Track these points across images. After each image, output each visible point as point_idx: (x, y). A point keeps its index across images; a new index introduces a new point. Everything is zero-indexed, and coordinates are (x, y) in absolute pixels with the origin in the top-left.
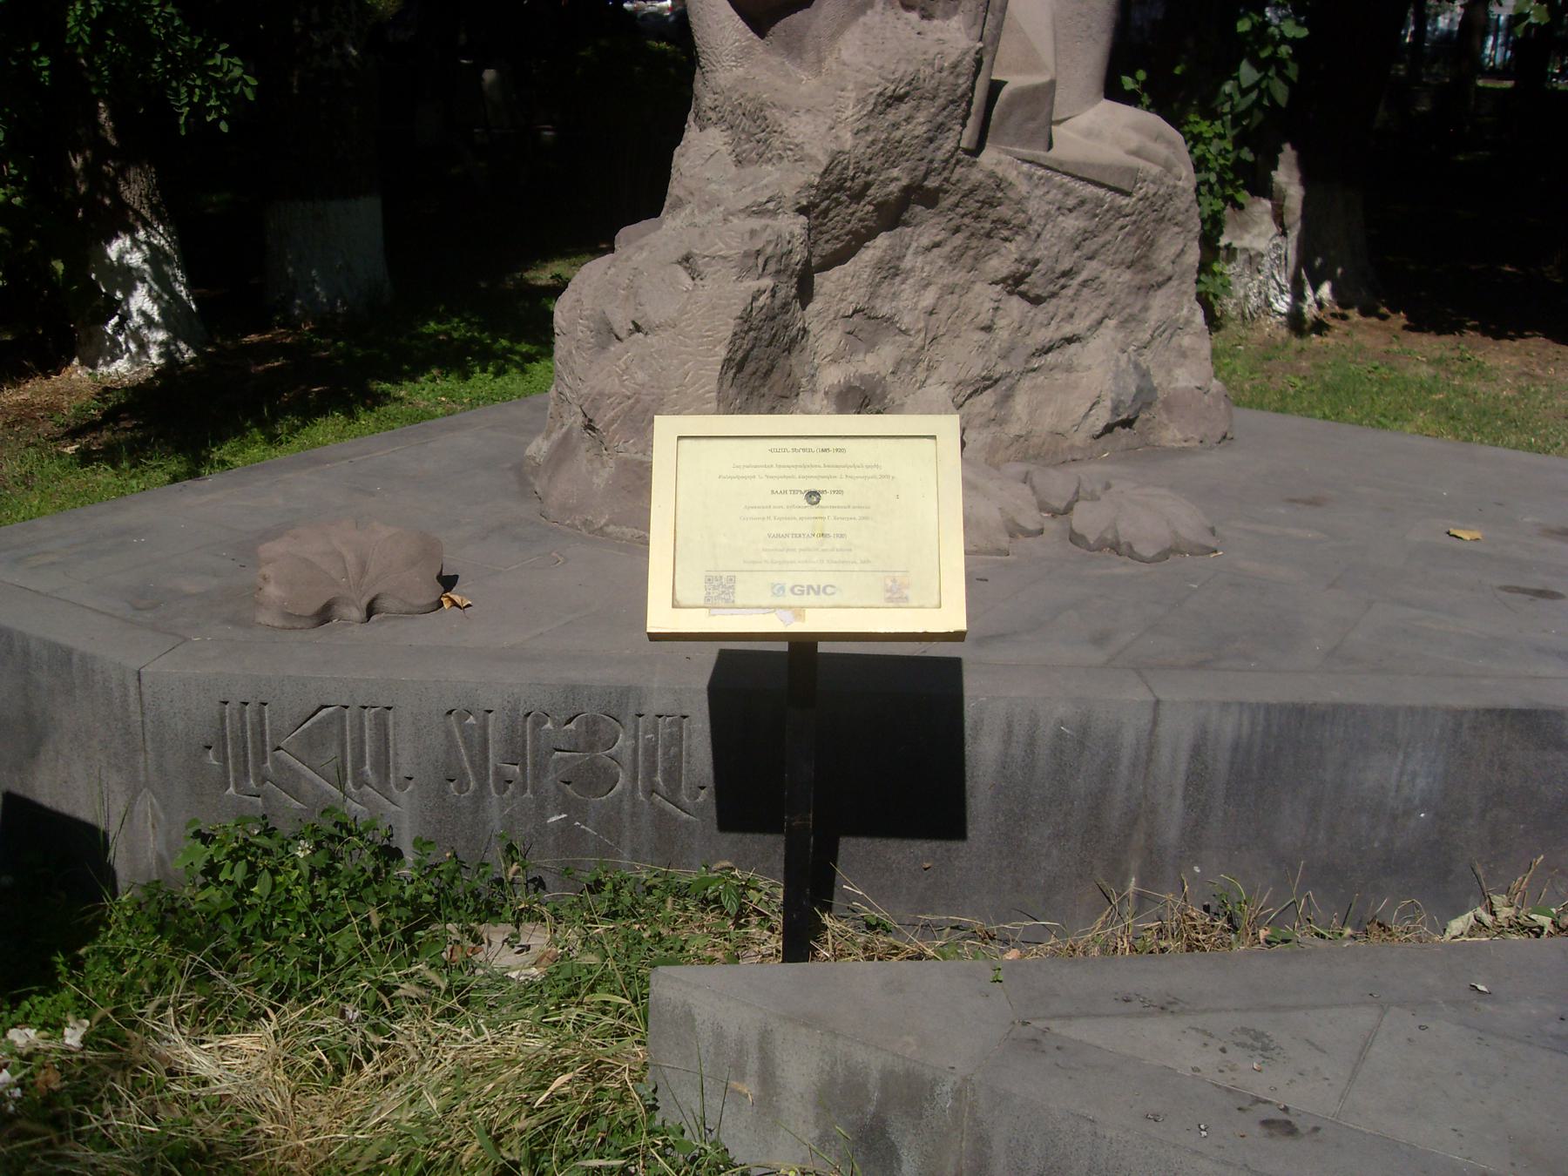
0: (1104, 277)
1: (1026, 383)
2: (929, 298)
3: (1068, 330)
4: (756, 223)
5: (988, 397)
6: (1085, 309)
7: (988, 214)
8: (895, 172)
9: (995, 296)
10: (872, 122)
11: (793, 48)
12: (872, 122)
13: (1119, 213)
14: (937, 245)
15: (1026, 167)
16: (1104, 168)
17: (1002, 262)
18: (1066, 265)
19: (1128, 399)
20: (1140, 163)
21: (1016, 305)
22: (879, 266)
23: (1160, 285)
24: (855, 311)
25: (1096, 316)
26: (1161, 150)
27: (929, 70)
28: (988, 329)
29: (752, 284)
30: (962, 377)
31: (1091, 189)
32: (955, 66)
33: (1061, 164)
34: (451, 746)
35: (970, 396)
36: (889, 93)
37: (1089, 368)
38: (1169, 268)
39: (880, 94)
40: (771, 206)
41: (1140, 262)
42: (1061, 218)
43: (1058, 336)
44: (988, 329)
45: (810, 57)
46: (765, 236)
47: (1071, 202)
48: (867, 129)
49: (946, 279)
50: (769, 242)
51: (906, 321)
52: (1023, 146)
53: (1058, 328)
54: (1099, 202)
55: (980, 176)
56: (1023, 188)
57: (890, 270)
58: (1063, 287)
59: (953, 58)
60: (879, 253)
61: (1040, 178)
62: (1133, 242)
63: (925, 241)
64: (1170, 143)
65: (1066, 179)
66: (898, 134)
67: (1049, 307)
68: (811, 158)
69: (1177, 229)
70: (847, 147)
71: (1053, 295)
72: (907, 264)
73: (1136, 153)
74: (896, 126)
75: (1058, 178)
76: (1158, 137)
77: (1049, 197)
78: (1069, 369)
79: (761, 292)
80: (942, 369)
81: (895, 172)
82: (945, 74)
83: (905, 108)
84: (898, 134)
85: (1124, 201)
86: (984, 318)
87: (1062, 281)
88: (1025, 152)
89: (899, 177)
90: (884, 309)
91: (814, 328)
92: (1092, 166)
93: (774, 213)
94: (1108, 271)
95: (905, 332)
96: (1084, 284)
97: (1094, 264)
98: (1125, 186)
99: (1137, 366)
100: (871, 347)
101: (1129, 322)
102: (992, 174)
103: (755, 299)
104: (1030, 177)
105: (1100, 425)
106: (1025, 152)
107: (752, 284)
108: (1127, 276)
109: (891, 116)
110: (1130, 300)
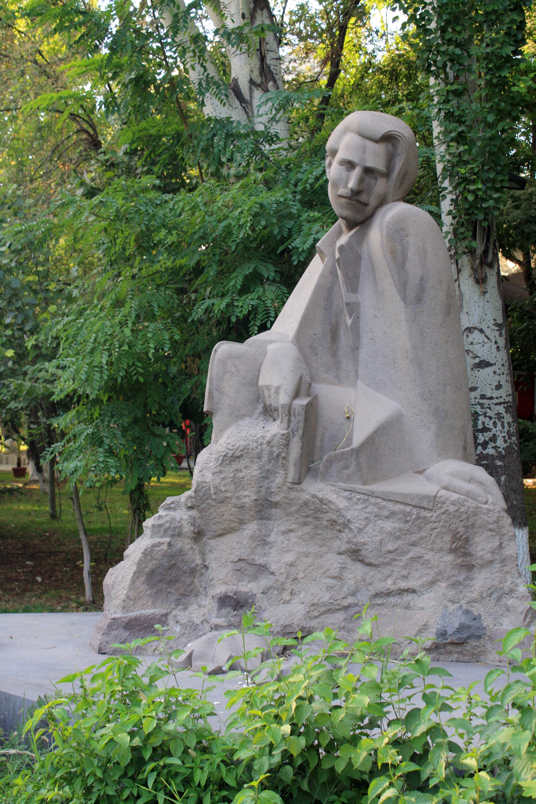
0: (426, 557)
2: (289, 558)
3: (403, 585)
5: (340, 616)
6: (417, 575)
8: (246, 493)
9: (341, 561)
10: (222, 469)
12: (222, 469)
14: (291, 531)
15: (346, 494)
16: (406, 496)
17: (340, 544)
18: (390, 547)
19: (450, 631)
20: (443, 492)
21: (358, 570)
22: (252, 538)
23: (483, 566)
24: (240, 560)
25: (426, 579)
27: (255, 445)
28: (338, 578)
30: (315, 601)
31: (402, 507)
32: (269, 443)
33: (373, 492)
35: (323, 614)
36: (230, 455)
37: (422, 609)
38: (488, 556)
39: (225, 456)
40: (173, 506)
42: (380, 522)
44: (338, 578)
46: (166, 519)
47: (385, 513)
48: (220, 472)
50: (167, 521)
51: (273, 568)
52: (344, 483)
53: (394, 583)
54: (407, 514)
55: (307, 497)
57: (262, 541)
58: (395, 560)
59: (268, 439)
60: (251, 532)
61: (359, 499)
62: (448, 538)
63: (283, 528)
64: (481, 483)
65: (379, 501)
66: (241, 475)
67: (387, 570)
69: (490, 533)
70: (208, 480)
71: (388, 564)
72: (271, 539)
73: (446, 488)
75: (373, 500)
76: (471, 480)
77: (368, 510)
78: (407, 607)
79: (159, 544)
80: (302, 595)
81: (246, 493)
82: (264, 446)
84: (241, 475)
85: (428, 514)
86: (334, 572)
87: (391, 556)
88: (346, 486)
89: (249, 496)
91: (213, 565)
92: (397, 494)
93: (174, 509)
94: (431, 554)
95: (272, 573)
96: (413, 559)
97: (418, 549)
99: (467, 612)
100: (255, 578)
102: (314, 496)
103: (154, 546)
105: (429, 644)
106: (346, 486)
107: (157, 540)
108: (450, 558)
109: (235, 466)
110: (456, 572)
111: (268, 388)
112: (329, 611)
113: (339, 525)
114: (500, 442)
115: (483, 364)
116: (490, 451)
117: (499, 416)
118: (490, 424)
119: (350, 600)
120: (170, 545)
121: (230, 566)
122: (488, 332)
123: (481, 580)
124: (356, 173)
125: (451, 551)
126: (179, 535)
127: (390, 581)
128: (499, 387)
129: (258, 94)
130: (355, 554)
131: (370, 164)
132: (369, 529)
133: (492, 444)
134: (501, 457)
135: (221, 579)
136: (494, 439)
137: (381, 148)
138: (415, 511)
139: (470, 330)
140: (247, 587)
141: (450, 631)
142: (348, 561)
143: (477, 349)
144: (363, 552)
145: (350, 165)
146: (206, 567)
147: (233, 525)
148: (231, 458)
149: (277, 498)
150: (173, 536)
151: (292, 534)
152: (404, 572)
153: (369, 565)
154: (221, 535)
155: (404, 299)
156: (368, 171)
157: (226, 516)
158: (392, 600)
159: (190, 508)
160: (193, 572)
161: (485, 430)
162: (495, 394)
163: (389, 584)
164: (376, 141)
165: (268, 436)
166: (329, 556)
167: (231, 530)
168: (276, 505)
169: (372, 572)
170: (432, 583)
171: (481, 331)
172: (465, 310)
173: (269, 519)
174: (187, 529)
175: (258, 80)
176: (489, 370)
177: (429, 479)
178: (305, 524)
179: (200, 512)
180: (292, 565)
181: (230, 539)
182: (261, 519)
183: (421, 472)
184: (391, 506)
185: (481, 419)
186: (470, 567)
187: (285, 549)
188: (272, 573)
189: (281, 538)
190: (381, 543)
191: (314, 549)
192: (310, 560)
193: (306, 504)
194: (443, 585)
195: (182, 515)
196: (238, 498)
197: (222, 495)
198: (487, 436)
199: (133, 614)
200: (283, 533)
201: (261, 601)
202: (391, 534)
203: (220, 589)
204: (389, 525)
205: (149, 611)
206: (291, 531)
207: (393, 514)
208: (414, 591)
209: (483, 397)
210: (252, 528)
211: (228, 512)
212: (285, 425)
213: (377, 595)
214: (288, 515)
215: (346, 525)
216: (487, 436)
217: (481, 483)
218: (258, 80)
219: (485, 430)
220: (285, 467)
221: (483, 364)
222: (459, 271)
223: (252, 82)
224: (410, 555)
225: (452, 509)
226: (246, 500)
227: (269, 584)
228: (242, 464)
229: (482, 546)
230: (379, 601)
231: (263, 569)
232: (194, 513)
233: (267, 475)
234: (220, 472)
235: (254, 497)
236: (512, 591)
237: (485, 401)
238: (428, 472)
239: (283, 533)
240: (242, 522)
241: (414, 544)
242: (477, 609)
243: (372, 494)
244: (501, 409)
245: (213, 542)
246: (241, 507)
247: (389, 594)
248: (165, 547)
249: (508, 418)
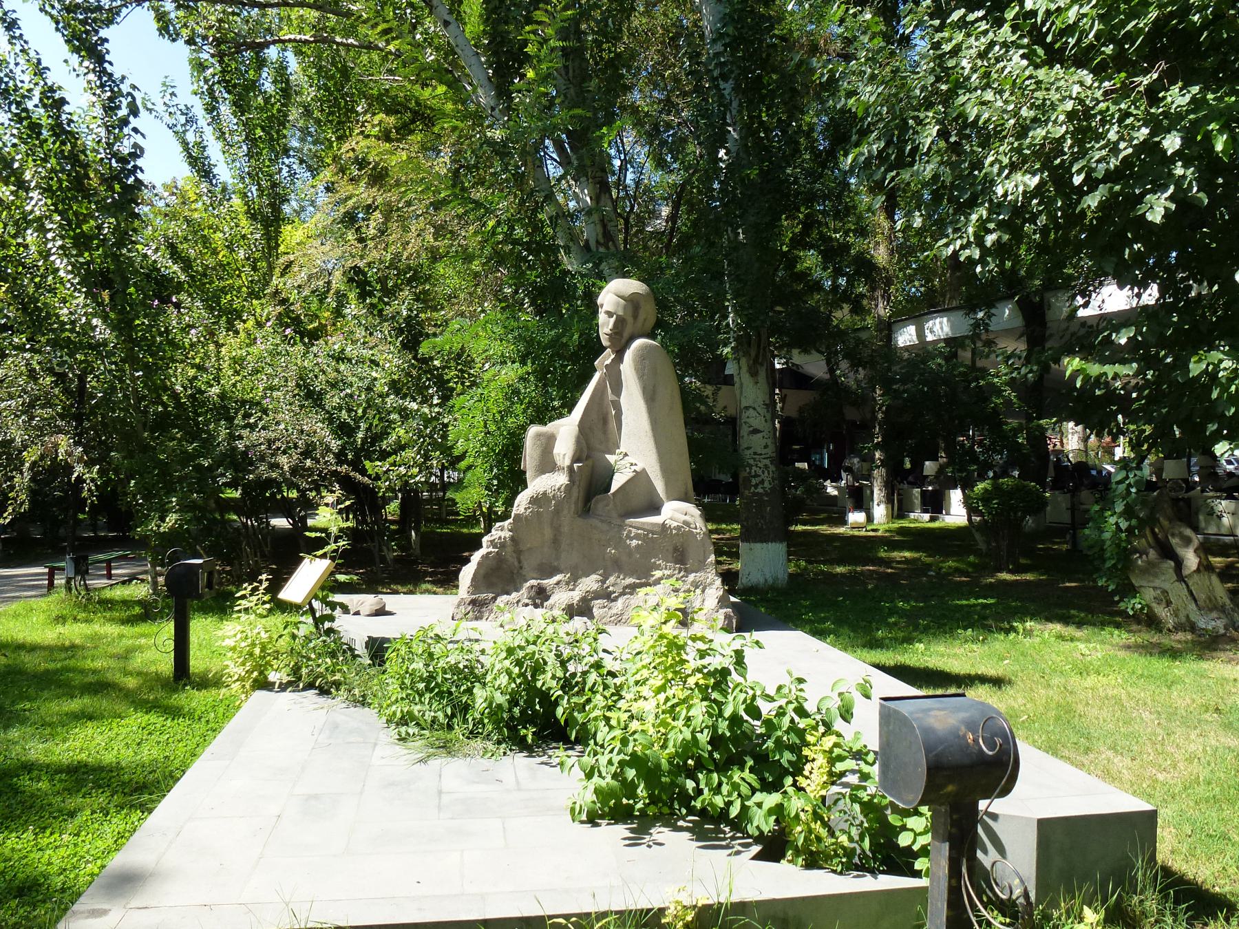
114: (766, 484)
115: (756, 431)
116: (760, 490)
117: (766, 466)
118: (760, 472)
122: (759, 409)
128: (766, 447)
134: (766, 494)
139: (747, 408)
143: (751, 421)
145: (610, 314)
161: (756, 476)
176: (760, 435)
198: (758, 480)
209: (755, 453)
216: (758, 480)
219: (756, 476)
221: (756, 431)
223: (597, 242)
236: (711, 584)
244: (767, 462)
249: (772, 468)
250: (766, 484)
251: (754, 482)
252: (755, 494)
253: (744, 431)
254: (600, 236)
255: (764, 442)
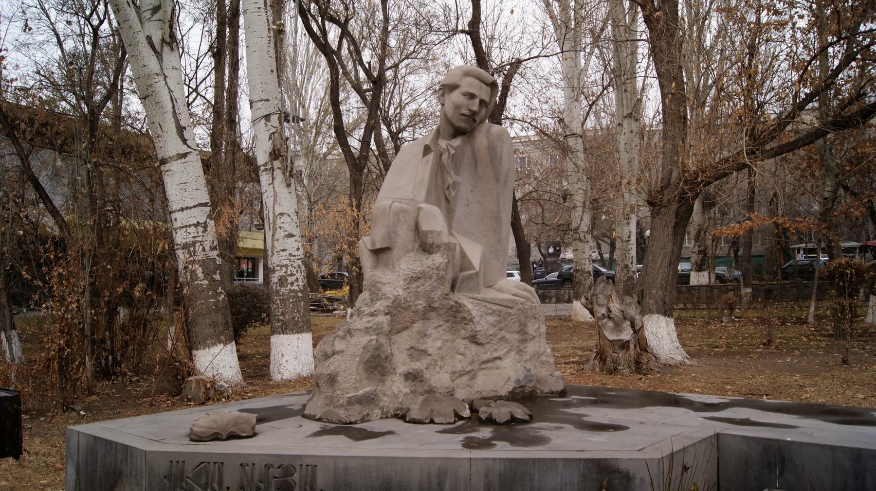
0: (507, 337)
1: (481, 373)
2: (439, 344)
3: (495, 355)
4: (370, 319)
5: (465, 378)
7: (456, 316)
8: (420, 302)
11: (386, 265)
13: (509, 313)
14: (440, 326)
16: (502, 300)
18: (491, 332)
20: (516, 298)
21: (474, 348)
22: (418, 332)
23: (531, 340)
25: (505, 350)
26: (526, 294)
29: (369, 338)
31: (498, 307)
32: (437, 268)
34: (241, 478)
38: (534, 334)
41: (522, 331)
43: (491, 357)
45: (391, 267)
47: (490, 311)
48: (408, 288)
49: (443, 338)
51: (430, 351)
54: (501, 311)
56: (470, 306)
57: (424, 335)
62: (517, 325)
64: (529, 292)
67: (487, 347)
68: (389, 298)
71: (488, 343)
73: (514, 295)
74: (418, 287)
75: (484, 304)
76: (525, 290)
78: (498, 368)
81: (420, 302)
83: (422, 281)
86: (462, 350)
87: (491, 338)
89: (421, 304)
90: (423, 348)
91: (396, 352)
93: (376, 315)
95: (430, 355)
97: (503, 332)
98: (510, 305)
99: (525, 367)
100: (418, 360)
101: (520, 352)
102: (457, 302)
104: (473, 303)
106: (470, 295)
107: (369, 338)
108: (517, 336)
111: (431, 232)
112: (461, 376)
113: (468, 320)
114: (300, 283)
115: (291, 235)
116: (295, 288)
119: (470, 368)
120: (377, 340)
121: (406, 352)
123: (531, 347)
124: (477, 101)
125: (518, 332)
126: (381, 333)
127: (489, 353)
128: (298, 249)
129: (166, 49)
130: (473, 339)
131: (484, 98)
132: (481, 322)
133: (296, 283)
135: (402, 363)
136: (297, 280)
137: (487, 89)
138: (505, 309)
139: (282, 214)
140: (417, 365)
141: (521, 379)
142: (468, 343)
144: (478, 337)
146: (392, 354)
147: (408, 324)
148: (415, 278)
149: (437, 305)
150: (378, 334)
151: (440, 328)
152: (496, 347)
153: (481, 344)
154: (400, 332)
155: (498, 181)
156: (482, 102)
157: (407, 319)
158: (490, 365)
159: (387, 314)
160: (387, 358)
162: (297, 253)
163: (488, 356)
164: (487, 84)
165: (438, 264)
166: (458, 340)
167: (407, 328)
168: (434, 309)
169: (480, 349)
170: (508, 352)
171: (289, 215)
172: (278, 202)
173: (428, 319)
174: (386, 328)
175: (168, 40)
176: (293, 239)
177: (500, 290)
178: (447, 321)
179: (391, 316)
180: (440, 348)
181: (405, 334)
182: (424, 319)
183: (490, 287)
184: (495, 307)
185: (290, 268)
186: (524, 341)
187: (436, 337)
188: (430, 355)
189: (434, 331)
190: (487, 330)
191: (448, 337)
192: (448, 344)
193: (451, 308)
194: (513, 353)
195: (383, 319)
196: (416, 306)
197: (407, 304)
199: (361, 392)
200: (436, 328)
201: (427, 375)
202: (491, 324)
203: (402, 369)
204: (491, 319)
205: (368, 389)
206: (440, 326)
207: (494, 311)
208: (500, 358)
209: (290, 255)
210: (418, 326)
211: (407, 316)
212: (445, 257)
213: (483, 363)
214: (439, 315)
215: (471, 320)
216: (293, 279)
217: (529, 292)
218: (168, 40)
219: (292, 275)
220: (443, 284)
221: (291, 235)
222: (273, 179)
223: (163, 40)
224: (499, 336)
225: (521, 306)
226: (420, 307)
227: (429, 362)
228: (418, 283)
229: (531, 328)
230: (483, 366)
231: (425, 352)
232: (388, 317)
233: (434, 289)
234: (408, 288)
235: (424, 305)
237: (292, 258)
238: (497, 286)
239: (436, 328)
240: (413, 322)
241: (501, 330)
242: (529, 365)
243: (484, 300)
244: (300, 262)
245: (395, 337)
246: (416, 312)
247: (488, 361)
248: (374, 342)
250: (300, 283)
251: (290, 279)
252: (291, 291)
253: (280, 234)
254: (168, 35)
255: (296, 245)
